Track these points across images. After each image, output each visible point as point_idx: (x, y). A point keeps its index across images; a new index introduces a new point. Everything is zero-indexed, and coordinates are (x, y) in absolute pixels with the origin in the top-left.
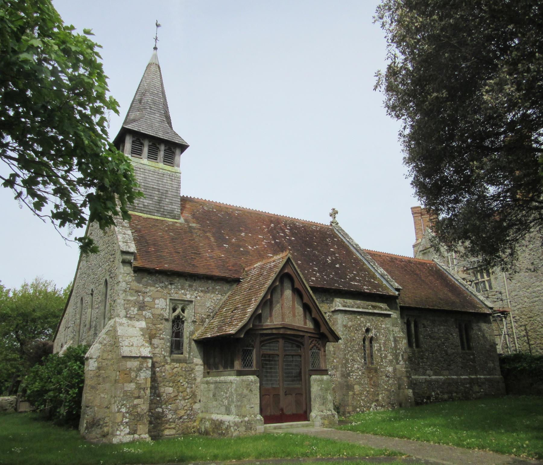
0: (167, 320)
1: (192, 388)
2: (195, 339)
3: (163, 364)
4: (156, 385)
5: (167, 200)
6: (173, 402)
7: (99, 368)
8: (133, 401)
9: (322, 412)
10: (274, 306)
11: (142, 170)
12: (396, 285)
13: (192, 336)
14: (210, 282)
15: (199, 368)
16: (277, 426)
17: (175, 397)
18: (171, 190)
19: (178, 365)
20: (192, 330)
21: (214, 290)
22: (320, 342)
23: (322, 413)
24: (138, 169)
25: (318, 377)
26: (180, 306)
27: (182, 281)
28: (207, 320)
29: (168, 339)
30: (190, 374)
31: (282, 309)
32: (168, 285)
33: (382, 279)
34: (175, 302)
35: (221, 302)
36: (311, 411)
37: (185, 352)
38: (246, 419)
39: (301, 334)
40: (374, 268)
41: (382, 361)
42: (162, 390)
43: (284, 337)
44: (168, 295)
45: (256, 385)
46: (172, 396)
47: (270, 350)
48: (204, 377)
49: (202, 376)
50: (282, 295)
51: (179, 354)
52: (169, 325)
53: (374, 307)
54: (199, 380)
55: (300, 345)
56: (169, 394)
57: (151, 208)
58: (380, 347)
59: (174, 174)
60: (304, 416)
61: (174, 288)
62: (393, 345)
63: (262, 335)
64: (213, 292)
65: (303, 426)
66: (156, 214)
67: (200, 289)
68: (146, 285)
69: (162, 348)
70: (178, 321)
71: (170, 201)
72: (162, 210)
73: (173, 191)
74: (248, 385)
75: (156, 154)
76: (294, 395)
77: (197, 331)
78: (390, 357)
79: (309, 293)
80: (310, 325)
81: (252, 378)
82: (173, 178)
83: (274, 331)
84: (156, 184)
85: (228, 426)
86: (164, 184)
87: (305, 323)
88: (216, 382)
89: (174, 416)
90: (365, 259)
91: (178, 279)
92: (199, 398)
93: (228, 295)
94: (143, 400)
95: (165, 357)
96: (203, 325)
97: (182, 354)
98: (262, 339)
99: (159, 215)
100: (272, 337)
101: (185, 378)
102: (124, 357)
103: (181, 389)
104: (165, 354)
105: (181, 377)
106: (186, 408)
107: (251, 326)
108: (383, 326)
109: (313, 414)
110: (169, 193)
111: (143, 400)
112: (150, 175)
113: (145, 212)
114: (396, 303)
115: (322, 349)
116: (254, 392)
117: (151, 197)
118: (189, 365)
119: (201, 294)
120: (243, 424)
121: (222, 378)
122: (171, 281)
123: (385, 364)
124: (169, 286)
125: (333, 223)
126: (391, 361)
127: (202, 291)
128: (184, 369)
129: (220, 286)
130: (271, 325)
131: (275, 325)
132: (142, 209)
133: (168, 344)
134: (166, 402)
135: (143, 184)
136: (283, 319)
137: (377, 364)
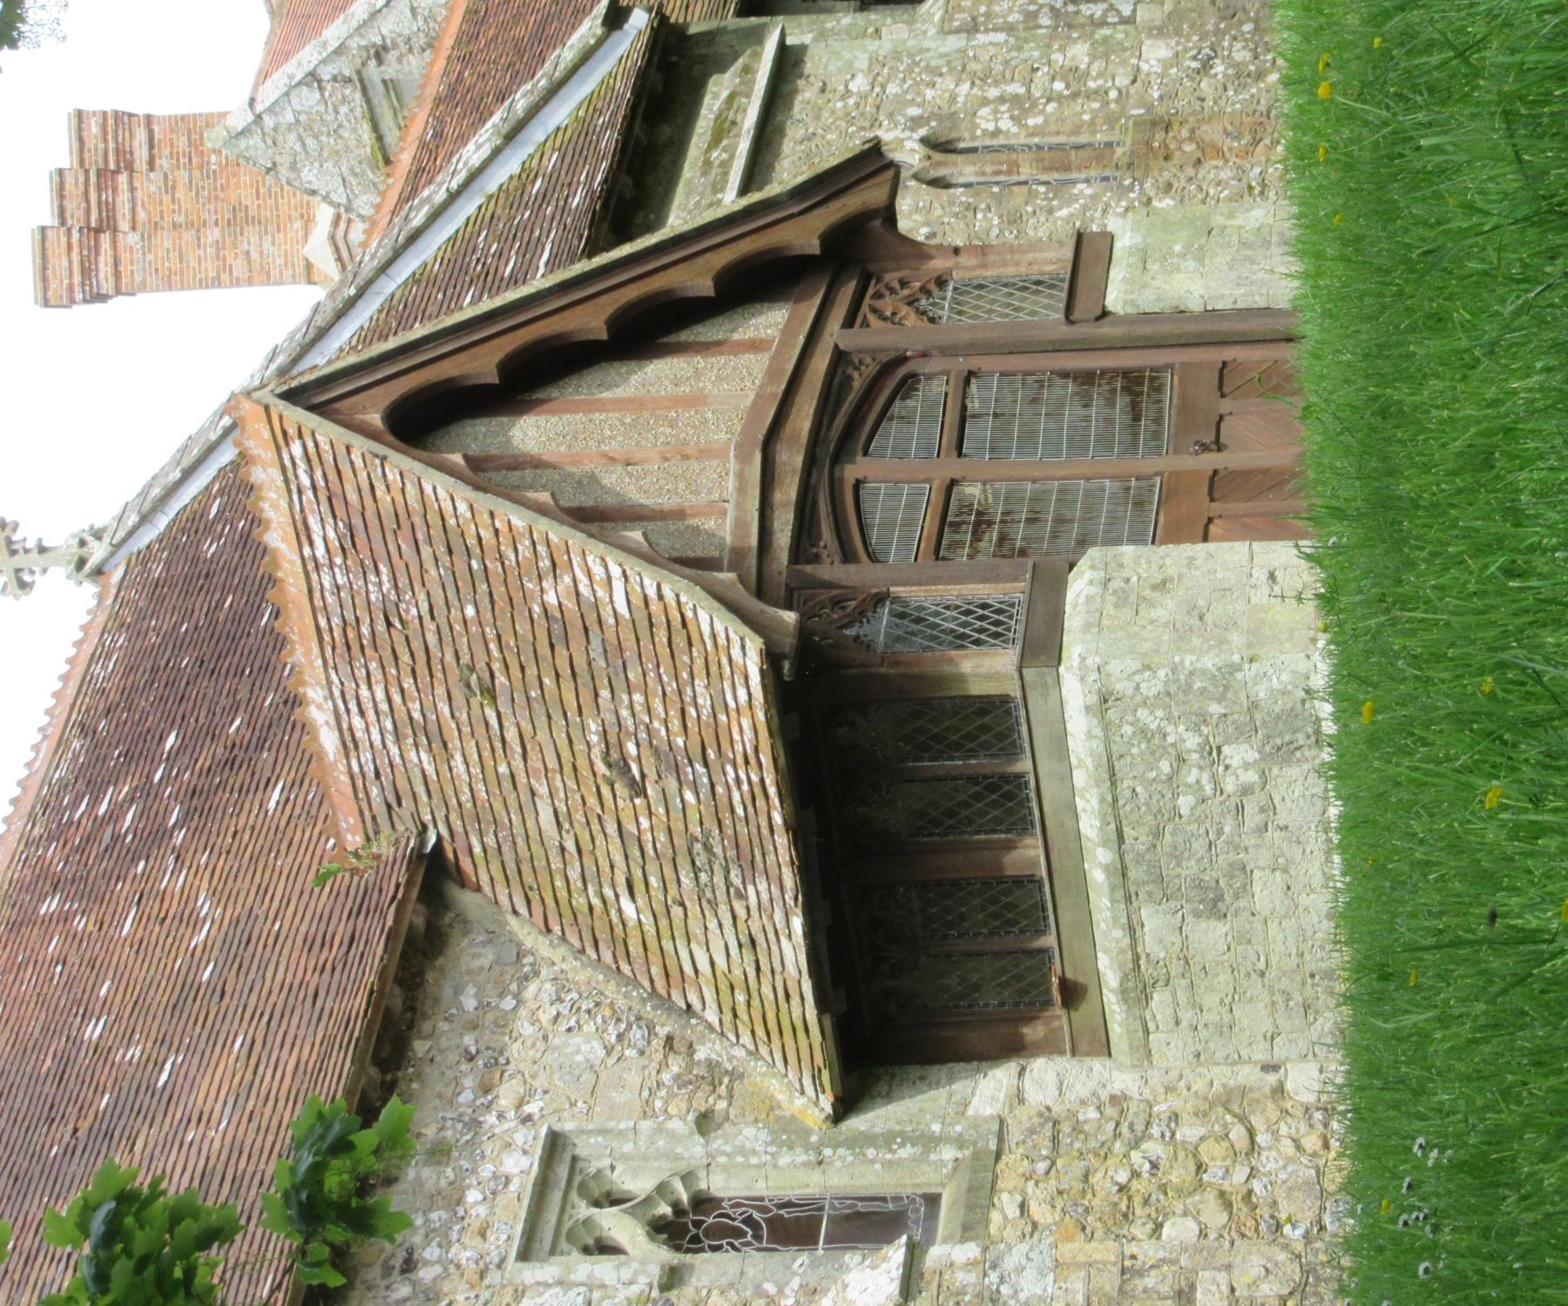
1: (1175, 1117)
2: (826, 1102)
6: (1265, 1212)
10: (609, 501)
12: (589, 27)
13: (808, 1132)
14: (420, 1047)
15: (1040, 1084)
17: (1228, 1205)
19: (1007, 1203)
20: (764, 1135)
22: (892, 278)
25: (1117, 274)
26: (583, 1210)
28: (701, 1054)
30: (1077, 1129)
33: (538, 133)
34: (547, 1234)
35: (582, 977)
37: (924, 1178)
39: (820, 364)
40: (453, 197)
41: (1101, 93)
44: (494, 1277)
45: (1127, 560)
48: (1105, 1048)
49: (1098, 1064)
52: (711, 1269)
53: (724, 128)
54: (1122, 1080)
55: (896, 377)
58: (1002, 99)
61: (446, 1245)
62: (1000, 37)
64: (503, 1024)
67: (466, 1096)
70: (689, 1225)
76: (1225, 406)
77: (772, 1106)
78: (1079, 53)
80: (771, 323)
81: (1080, 587)
83: (787, 493)
90: (384, 269)
92: (1248, 1075)
93: (525, 933)
94: (1205, 1275)
96: (735, 1075)
97: (933, 1200)
100: (824, 509)
108: (859, 84)
111: (1205, 1275)
114: (709, 37)
115: (938, 264)
116: (1172, 571)
118: (1014, 1135)
119: (506, 1095)
121: (1090, 825)
123: (1122, 80)
124: (426, 1274)
125: (81, 563)
126: (1104, 50)
128: (1042, 1166)
129: (458, 991)
130: (739, 506)
131: (741, 489)
137: (1111, 120)
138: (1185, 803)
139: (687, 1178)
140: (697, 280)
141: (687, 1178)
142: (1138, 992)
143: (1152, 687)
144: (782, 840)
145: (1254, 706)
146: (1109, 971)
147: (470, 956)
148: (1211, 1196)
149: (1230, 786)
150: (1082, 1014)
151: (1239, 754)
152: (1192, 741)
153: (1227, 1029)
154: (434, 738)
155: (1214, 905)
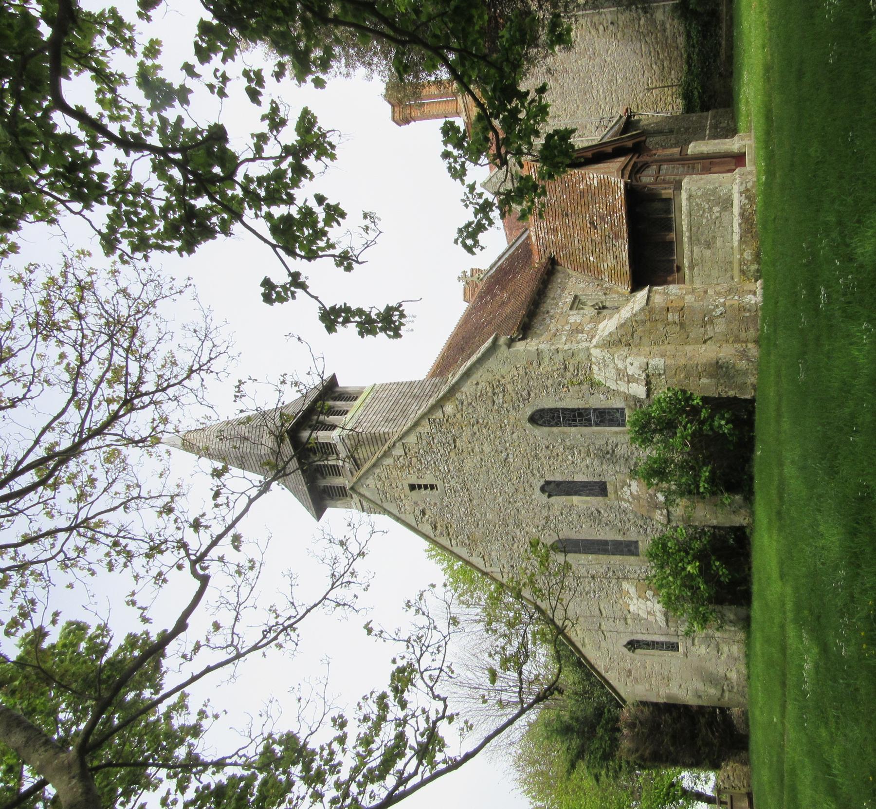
2: (629, 290)
7: (662, 356)
8: (711, 296)
39: (632, 163)
64: (566, 283)
68: (547, 329)
85: (746, 197)
88: (690, 238)
93: (570, 271)
102: (647, 304)
121: (685, 228)
138: (704, 221)
139: (602, 302)
140: (609, 149)
141: (602, 302)
142: (692, 268)
143: (699, 194)
144: (625, 227)
145: (720, 197)
146: (686, 263)
147: (559, 278)
149: (714, 217)
150: (681, 273)
151: (716, 209)
152: (707, 206)
153: (709, 276)
154: (555, 231)
155: (709, 246)
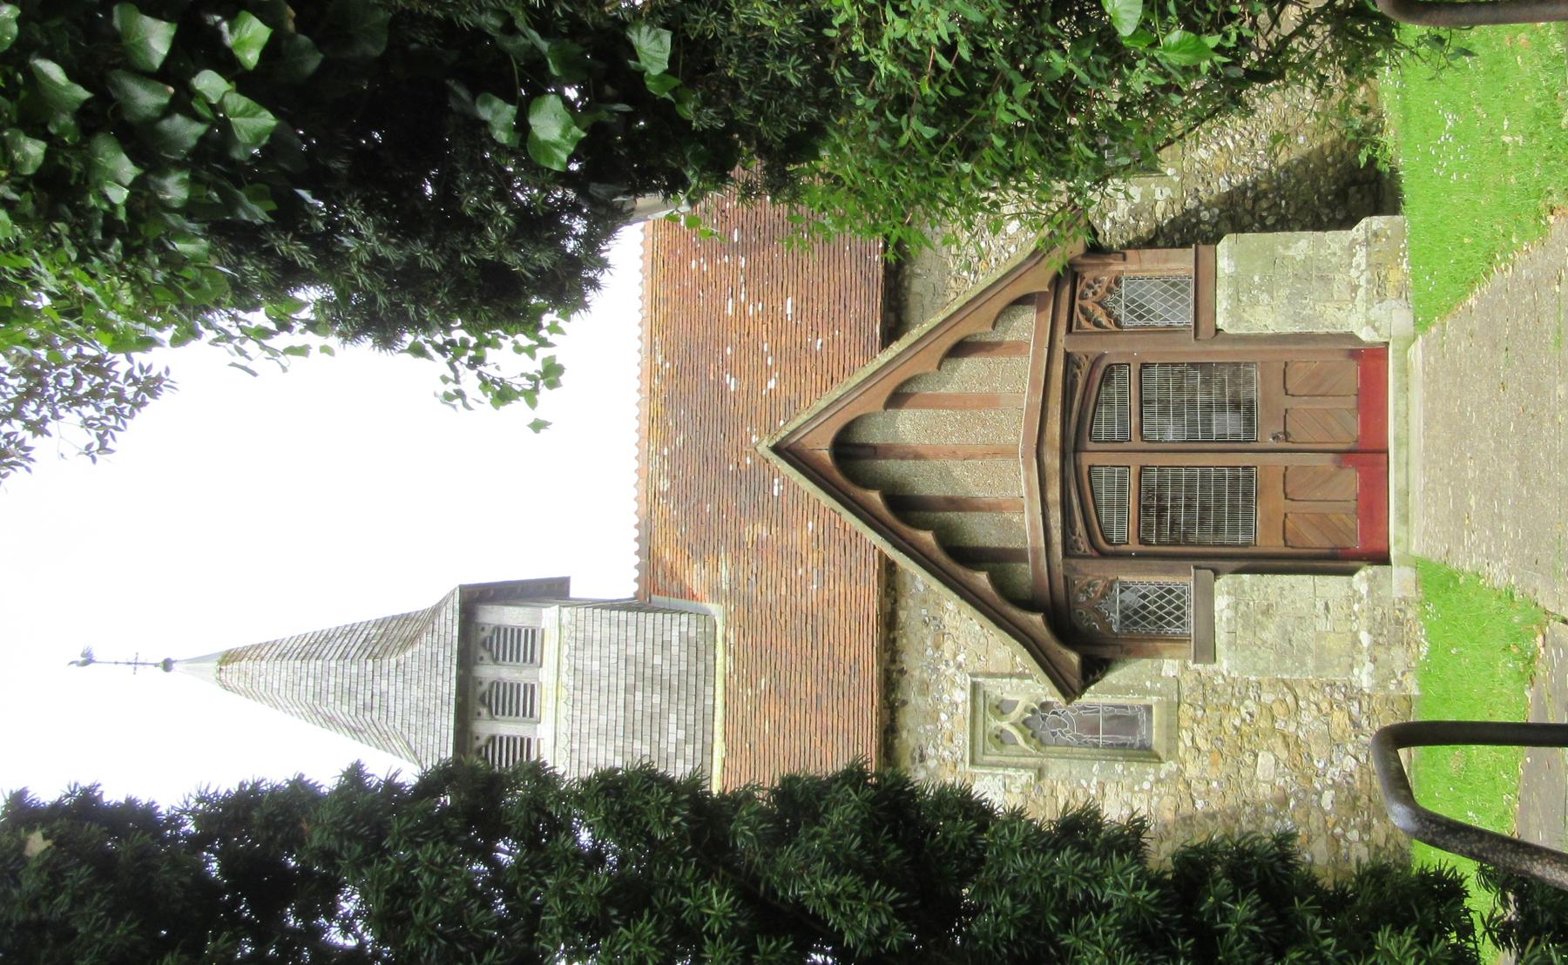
0: (1041, 773)
3: (1181, 787)
4: (1248, 810)
5: (658, 660)
6: (1304, 749)
9: (1355, 288)
10: (960, 492)
11: (576, 746)
16: (1397, 509)
17: (1288, 745)
18: (622, 647)
19: (1186, 735)
21: (931, 598)
23: (1361, 292)
24: (575, 755)
25: (1223, 304)
27: (907, 719)
29: (1102, 770)
31: (971, 457)
32: (926, 768)
36: (1351, 337)
38: (1365, 639)
42: (1264, 790)
43: (1071, 448)
44: (960, 767)
46: (1284, 755)
47: (1121, 505)
50: (918, 456)
51: (1150, 720)
56: (1277, 763)
57: (691, 718)
59: (565, 633)
60: (1371, 360)
63: (1069, 549)
65: (1405, 389)
66: (709, 702)
67: (929, 652)
69: (1131, 790)
71: (658, 649)
72: (692, 680)
73: (623, 637)
74: (1250, 620)
75: (514, 687)
79: (899, 355)
82: (580, 635)
83: (1054, 494)
84: (612, 697)
86: (605, 671)
87: (1018, 348)
89: (1350, 747)
91: (904, 734)
95: (1159, 781)
97: (1149, 709)
98: (1084, 546)
99: (709, 690)
100: (1075, 501)
101: (1228, 707)
103: (1263, 724)
104: (1151, 778)
105: (1225, 723)
106: (1325, 706)
107: (1037, 619)
109: (1366, 335)
110: (631, 652)
112: (586, 716)
113: (708, 739)
117: (656, 719)
119: (948, 646)
120: (1381, 654)
122: (913, 759)
124: (932, 763)
127: (937, 647)
131: (1030, 494)
132: (699, 746)
133: (1119, 767)
134: (1304, 776)
135: (620, 743)
136: (1007, 453)
148: (1280, 741)
